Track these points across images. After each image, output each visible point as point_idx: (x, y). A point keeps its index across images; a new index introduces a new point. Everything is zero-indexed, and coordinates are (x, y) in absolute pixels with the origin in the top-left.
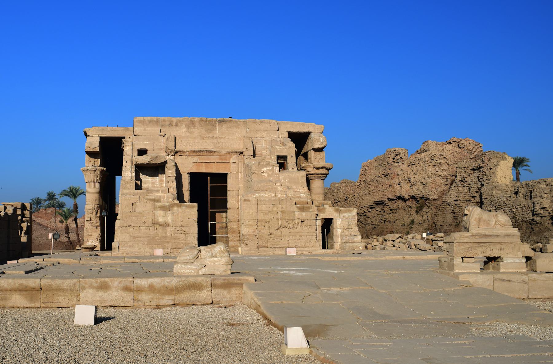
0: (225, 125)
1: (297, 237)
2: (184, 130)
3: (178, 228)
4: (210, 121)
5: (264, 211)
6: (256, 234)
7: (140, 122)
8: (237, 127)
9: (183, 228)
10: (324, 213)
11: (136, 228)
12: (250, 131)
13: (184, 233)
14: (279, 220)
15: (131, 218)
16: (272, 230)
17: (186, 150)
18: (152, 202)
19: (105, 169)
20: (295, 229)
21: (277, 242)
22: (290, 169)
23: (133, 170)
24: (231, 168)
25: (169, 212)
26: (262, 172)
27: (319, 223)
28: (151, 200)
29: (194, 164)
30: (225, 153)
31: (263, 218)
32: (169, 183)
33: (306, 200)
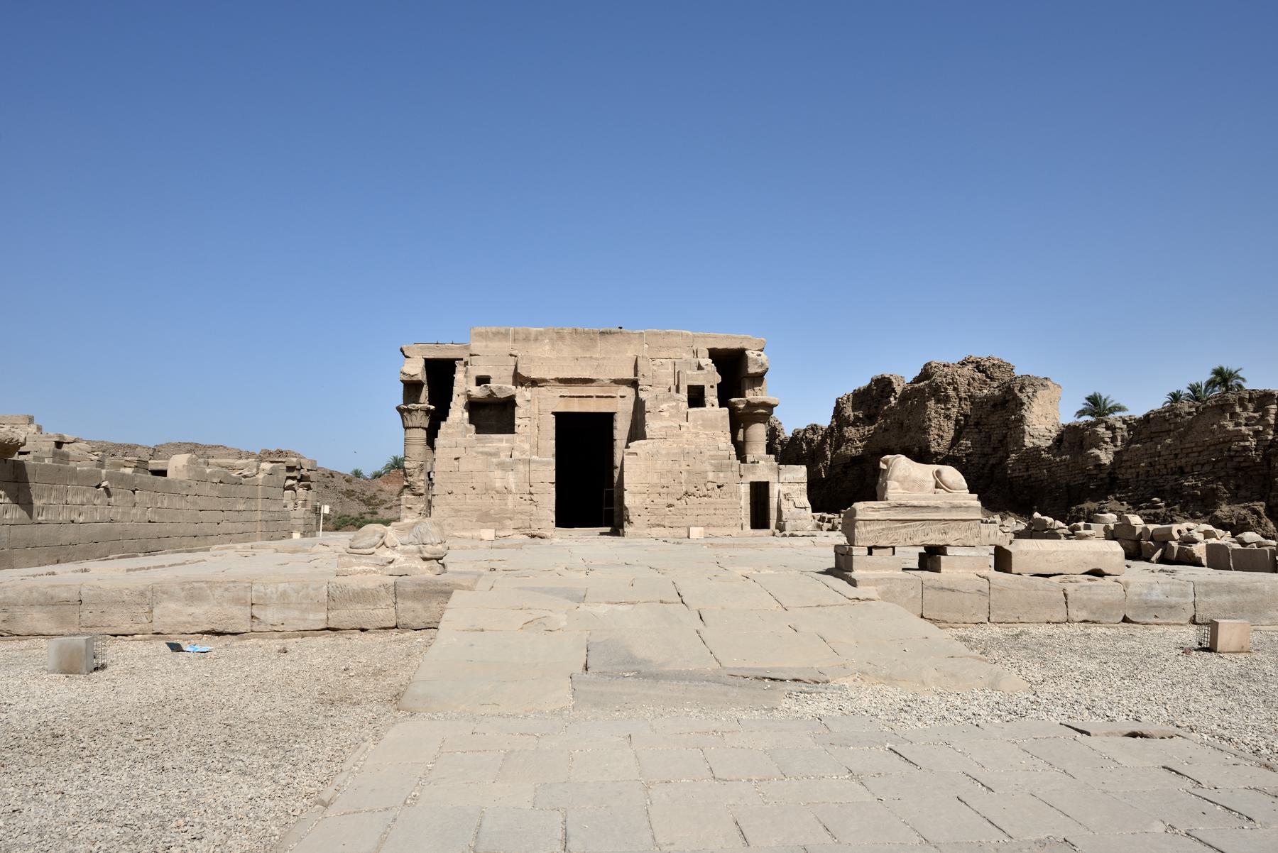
0: (611, 339)
2: (547, 348)
5: (658, 471)
7: (480, 335)
10: (754, 473)
11: (460, 497)
13: (534, 504)
14: (683, 484)
15: (452, 481)
17: (548, 377)
18: (486, 457)
19: (432, 407)
20: (706, 499)
21: (678, 519)
22: (708, 406)
24: (619, 405)
25: (510, 473)
26: (661, 410)
27: (745, 490)
28: (482, 453)
30: (609, 381)
31: (658, 481)
32: (520, 428)
33: (727, 453)
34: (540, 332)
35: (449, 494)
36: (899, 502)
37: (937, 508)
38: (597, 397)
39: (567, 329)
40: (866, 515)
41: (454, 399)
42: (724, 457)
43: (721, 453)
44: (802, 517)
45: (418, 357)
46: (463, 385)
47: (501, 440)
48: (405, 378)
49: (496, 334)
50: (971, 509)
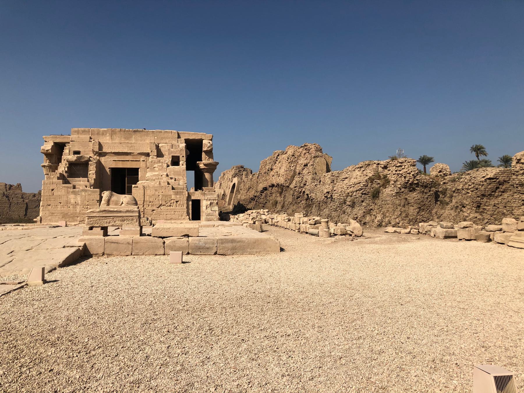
1: (173, 213)
2: (108, 138)
3: (85, 207)
4: (127, 131)
6: (143, 211)
8: (147, 136)
9: (89, 207)
10: (194, 196)
11: (53, 207)
12: (157, 138)
15: (50, 200)
16: (154, 208)
23: (68, 165)
25: (78, 196)
29: (113, 161)
30: (136, 154)
34: (105, 130)
35: (50, 205)
36: (104, 209)
37: (120, 212)
38: (131, 161)
39: (117, 129)
40: (90, 214)
41: (62, 161)
42: (181, 189)
43: (179, 186)
44: (214, 215)
45: (51, 141)
46: (68, 156)
47: (80, 181)
48: (43, 151)
49: (84, 132)
50: (134, 212)
